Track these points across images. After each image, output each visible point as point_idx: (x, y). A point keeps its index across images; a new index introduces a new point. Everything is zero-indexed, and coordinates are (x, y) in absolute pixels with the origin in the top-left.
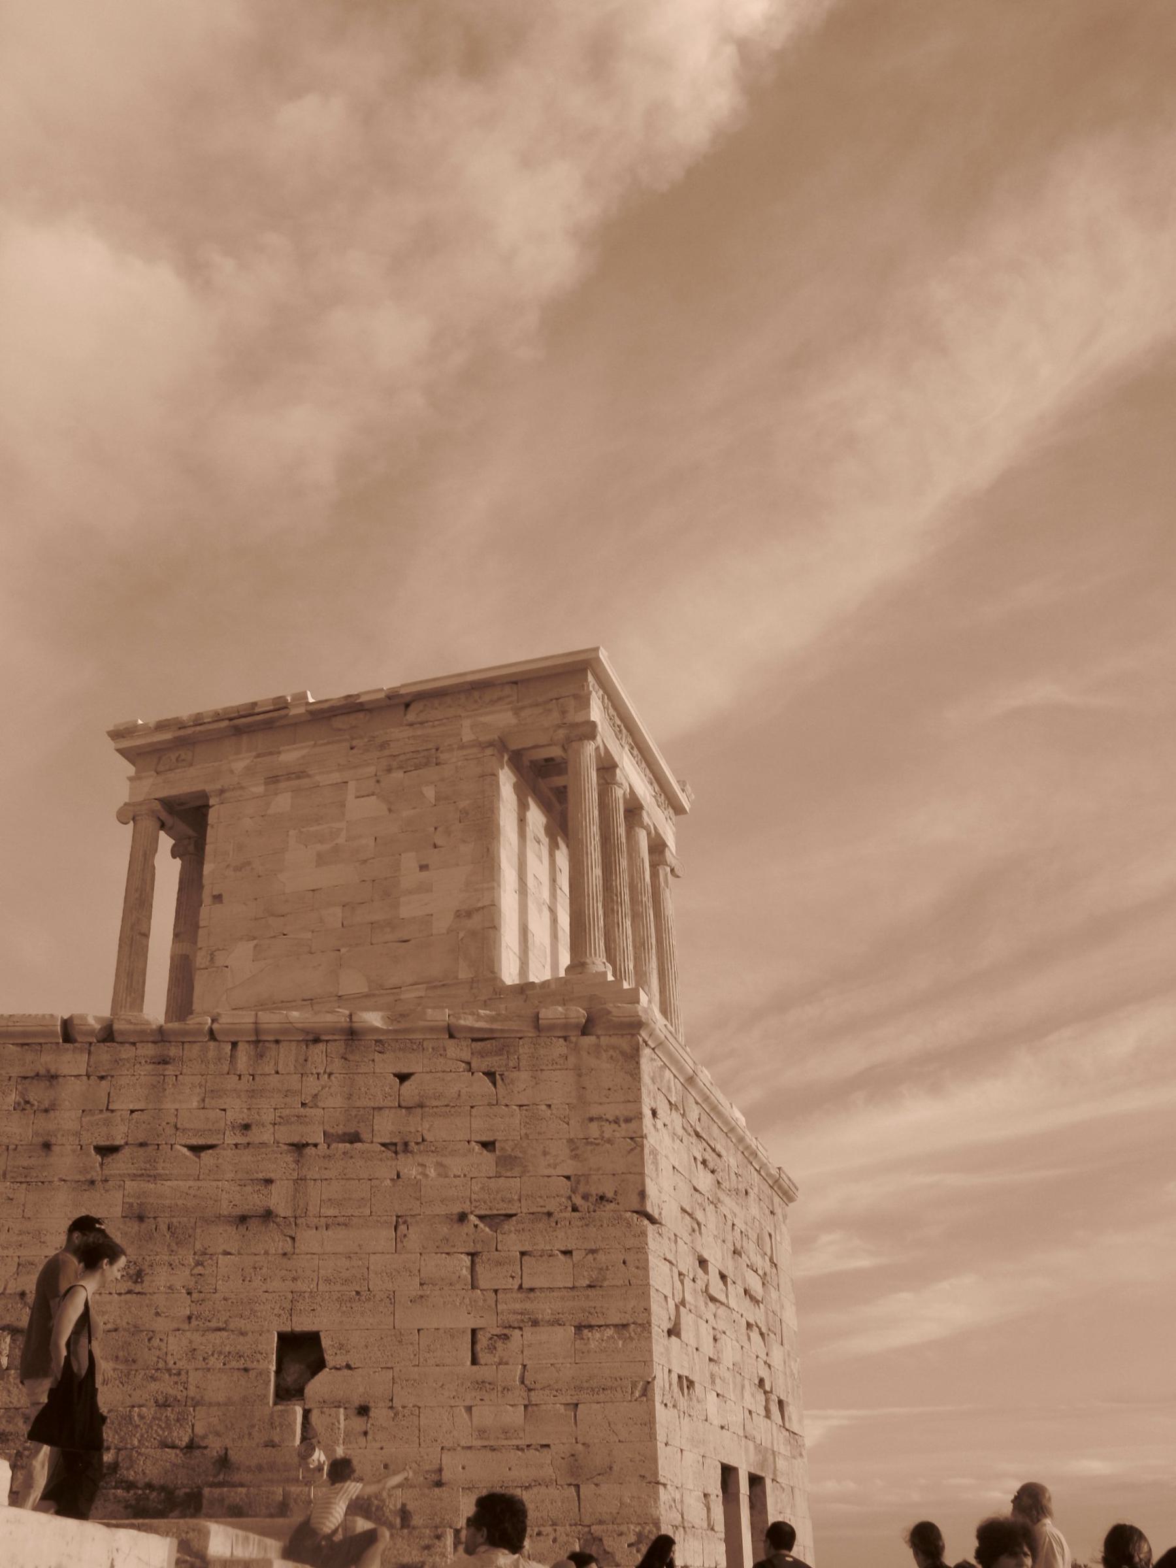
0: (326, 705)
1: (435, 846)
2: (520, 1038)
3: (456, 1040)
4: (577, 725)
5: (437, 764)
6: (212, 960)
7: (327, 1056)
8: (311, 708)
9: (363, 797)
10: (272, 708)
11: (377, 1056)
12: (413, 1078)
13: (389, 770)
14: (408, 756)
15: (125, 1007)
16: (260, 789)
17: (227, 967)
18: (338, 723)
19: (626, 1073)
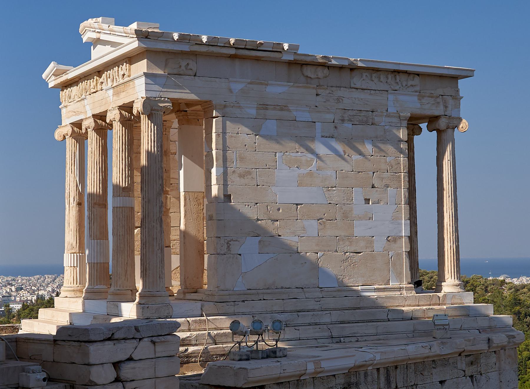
0: (308, 59)
1: (373, 187)
2: (481, 353)
3: (460, 357)
4: (453, 118)
5: (372, 124)
6: (228, 247)
7: (415, 373)
8: (298, 58)
9: (326, 137)
10: (271, 49)
11: (434, 371)
12: (446, 382)
13: (343, 120)
14: (354, 113)
15: (162, 278)
16: (253, 112)
17: (240, 255)
18: (309, 71)
19: (514, 371)
